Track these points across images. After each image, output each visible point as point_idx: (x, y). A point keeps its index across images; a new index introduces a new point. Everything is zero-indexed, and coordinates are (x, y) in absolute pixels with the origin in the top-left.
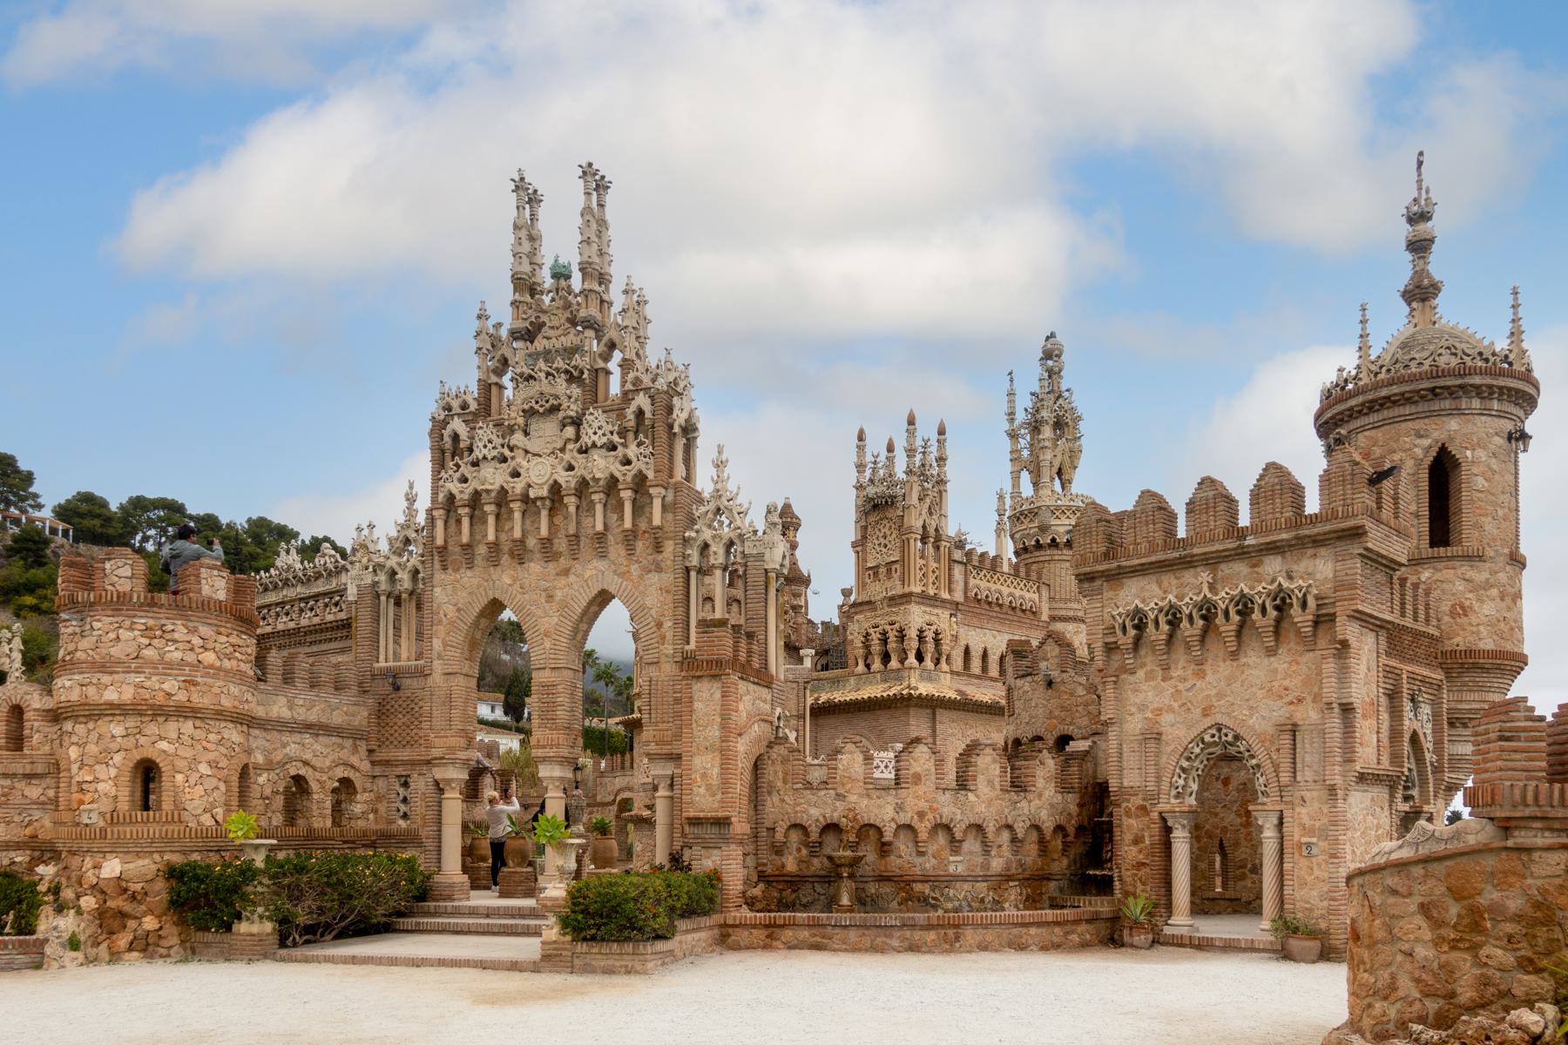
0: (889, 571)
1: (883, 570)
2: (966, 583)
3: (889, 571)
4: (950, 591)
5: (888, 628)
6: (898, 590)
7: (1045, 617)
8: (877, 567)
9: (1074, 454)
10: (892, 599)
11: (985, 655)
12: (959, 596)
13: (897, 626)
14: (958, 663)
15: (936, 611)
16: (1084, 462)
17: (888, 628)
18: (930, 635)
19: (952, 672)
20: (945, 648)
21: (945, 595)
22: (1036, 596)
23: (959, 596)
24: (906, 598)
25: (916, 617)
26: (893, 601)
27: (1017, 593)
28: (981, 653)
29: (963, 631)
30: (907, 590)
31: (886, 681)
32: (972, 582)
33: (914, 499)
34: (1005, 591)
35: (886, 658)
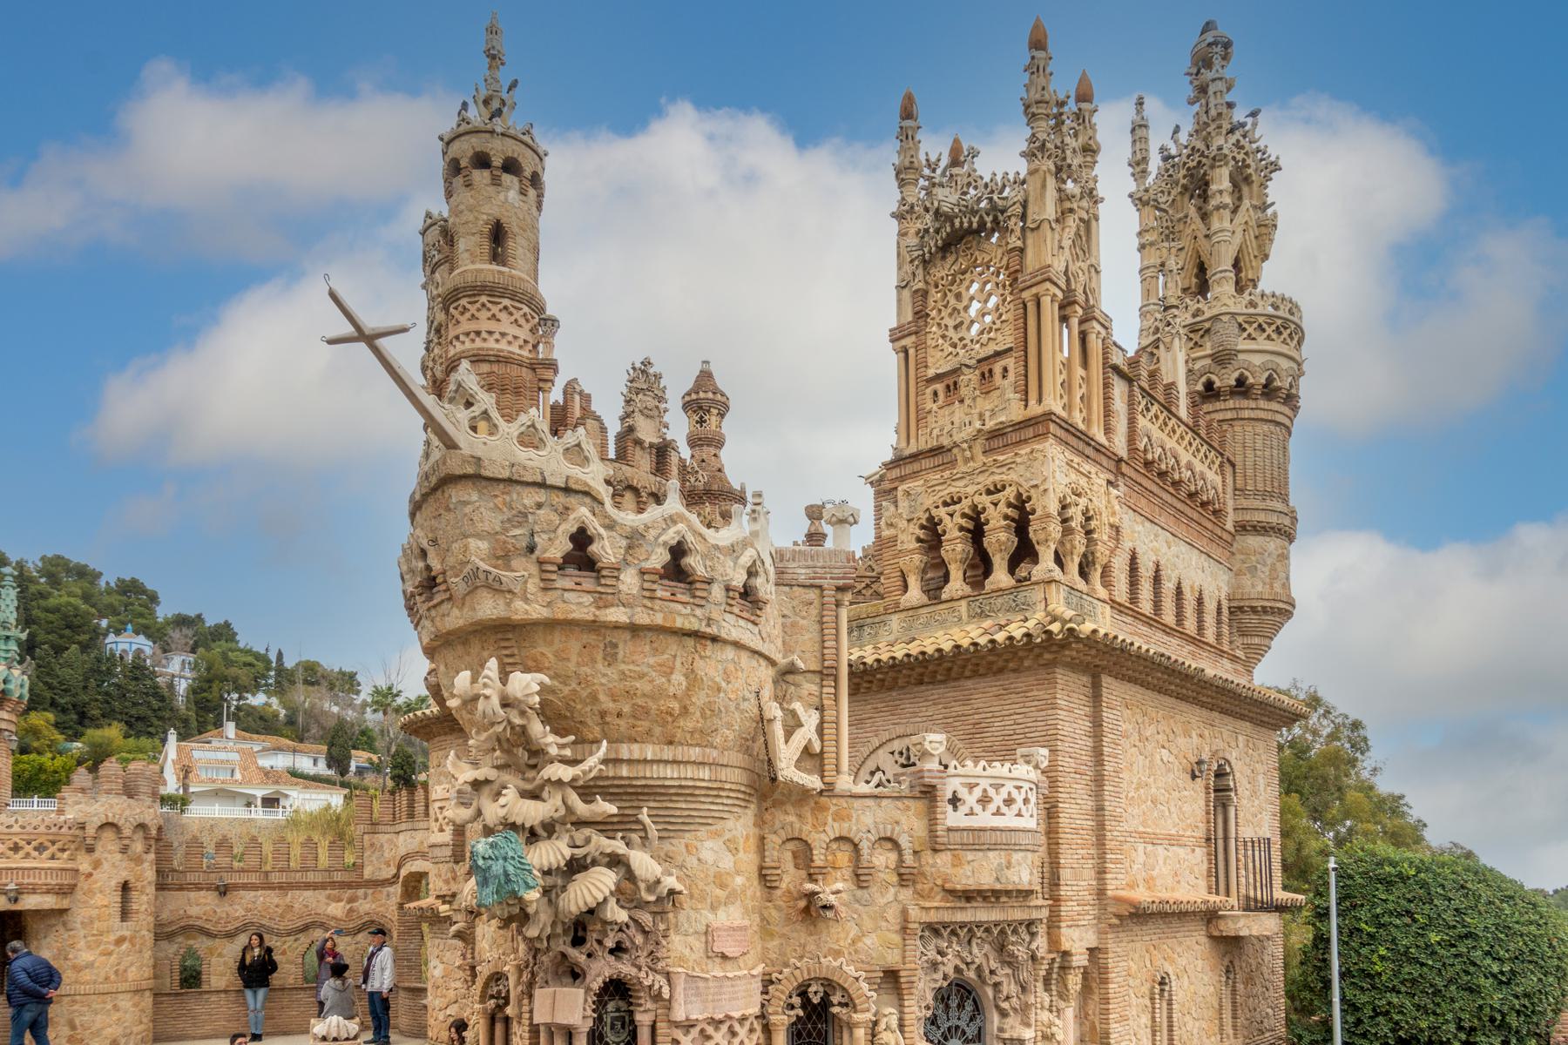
0: (987, 376)
1: (970, 378)
2: (1132, 421)
3: (987, 376)
4: (1108, 430)
5: (985, 500)
6: (1015, 412)
7: (1229, 526)
8: (955, 371)
9: (1265, 230)
10: (996, 434)
11: (1157, 579)
12: (1120, 446)
13: (1010, 493)
14: (1121, 592)
15: (1086, 467)
16: (1283, 244)
17: (985, 500)
18: (1076, 513)
19: (1114, 604)
20: (1102, 552)
21: (1101, 438)
22: (1218, 479)
23: (1120, 446)
24: (1037, 426)
25: (1054, 473)
26: (998, 438)
27: (1199, 467)
28: (1151, 573)
29: (1127, 520)
30: (1035, 409)
31: (982, 615)
32: (1142, 422)
33: (1050, 211)
34: (1185, 457)
35: (981, 564)
